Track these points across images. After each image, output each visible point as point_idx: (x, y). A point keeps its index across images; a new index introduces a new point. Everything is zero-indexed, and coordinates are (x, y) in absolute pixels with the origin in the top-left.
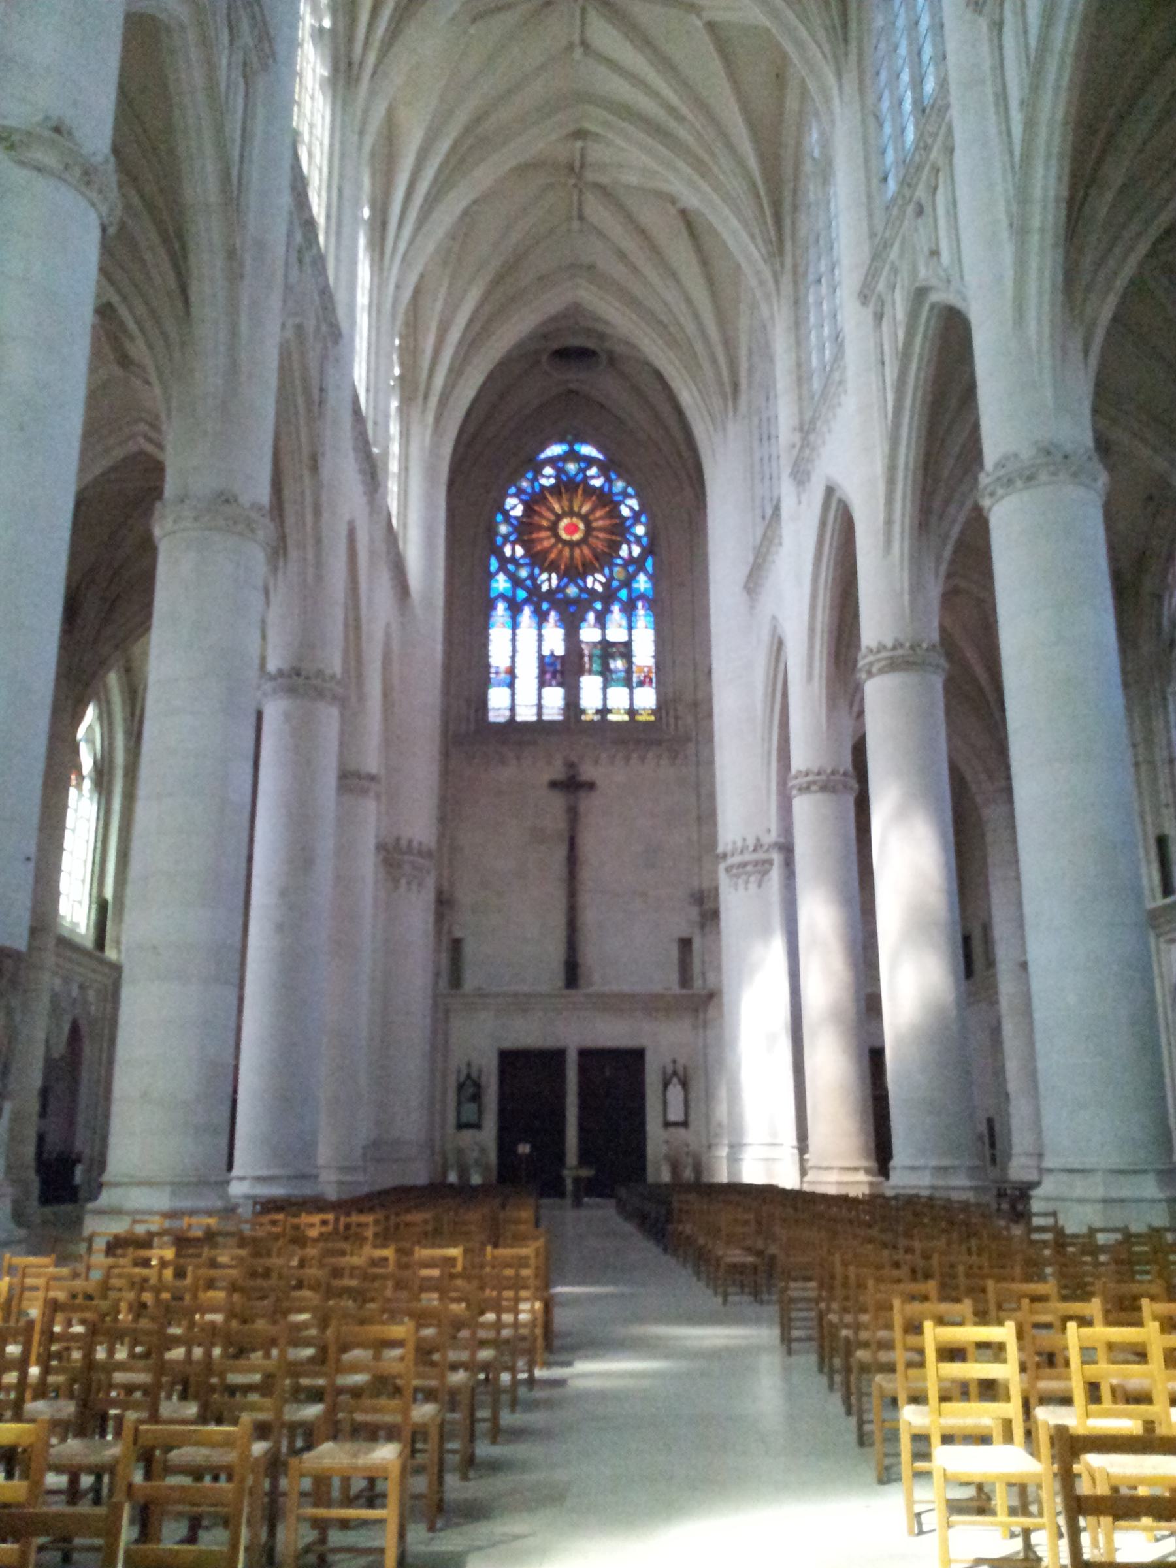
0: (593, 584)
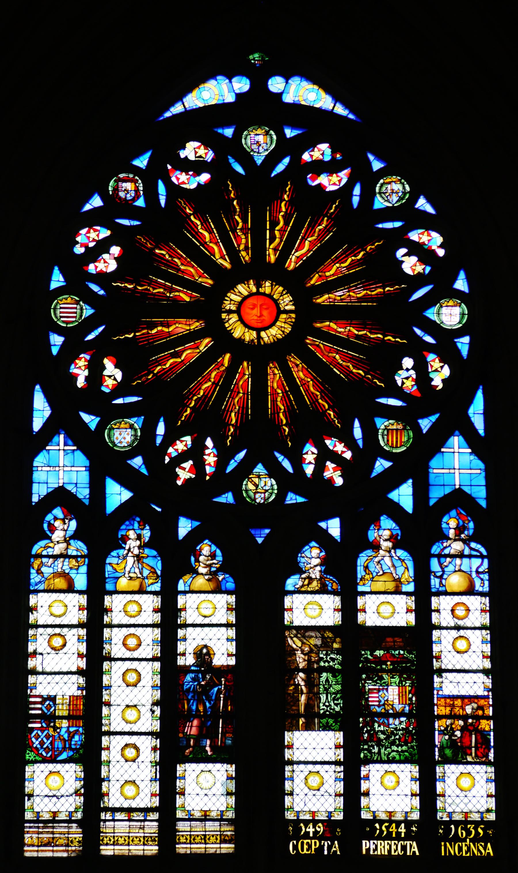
0: (320, 467)
